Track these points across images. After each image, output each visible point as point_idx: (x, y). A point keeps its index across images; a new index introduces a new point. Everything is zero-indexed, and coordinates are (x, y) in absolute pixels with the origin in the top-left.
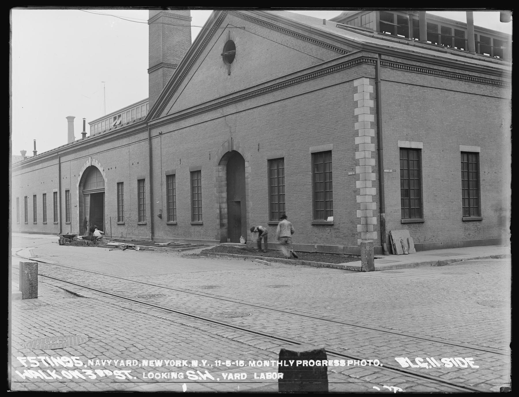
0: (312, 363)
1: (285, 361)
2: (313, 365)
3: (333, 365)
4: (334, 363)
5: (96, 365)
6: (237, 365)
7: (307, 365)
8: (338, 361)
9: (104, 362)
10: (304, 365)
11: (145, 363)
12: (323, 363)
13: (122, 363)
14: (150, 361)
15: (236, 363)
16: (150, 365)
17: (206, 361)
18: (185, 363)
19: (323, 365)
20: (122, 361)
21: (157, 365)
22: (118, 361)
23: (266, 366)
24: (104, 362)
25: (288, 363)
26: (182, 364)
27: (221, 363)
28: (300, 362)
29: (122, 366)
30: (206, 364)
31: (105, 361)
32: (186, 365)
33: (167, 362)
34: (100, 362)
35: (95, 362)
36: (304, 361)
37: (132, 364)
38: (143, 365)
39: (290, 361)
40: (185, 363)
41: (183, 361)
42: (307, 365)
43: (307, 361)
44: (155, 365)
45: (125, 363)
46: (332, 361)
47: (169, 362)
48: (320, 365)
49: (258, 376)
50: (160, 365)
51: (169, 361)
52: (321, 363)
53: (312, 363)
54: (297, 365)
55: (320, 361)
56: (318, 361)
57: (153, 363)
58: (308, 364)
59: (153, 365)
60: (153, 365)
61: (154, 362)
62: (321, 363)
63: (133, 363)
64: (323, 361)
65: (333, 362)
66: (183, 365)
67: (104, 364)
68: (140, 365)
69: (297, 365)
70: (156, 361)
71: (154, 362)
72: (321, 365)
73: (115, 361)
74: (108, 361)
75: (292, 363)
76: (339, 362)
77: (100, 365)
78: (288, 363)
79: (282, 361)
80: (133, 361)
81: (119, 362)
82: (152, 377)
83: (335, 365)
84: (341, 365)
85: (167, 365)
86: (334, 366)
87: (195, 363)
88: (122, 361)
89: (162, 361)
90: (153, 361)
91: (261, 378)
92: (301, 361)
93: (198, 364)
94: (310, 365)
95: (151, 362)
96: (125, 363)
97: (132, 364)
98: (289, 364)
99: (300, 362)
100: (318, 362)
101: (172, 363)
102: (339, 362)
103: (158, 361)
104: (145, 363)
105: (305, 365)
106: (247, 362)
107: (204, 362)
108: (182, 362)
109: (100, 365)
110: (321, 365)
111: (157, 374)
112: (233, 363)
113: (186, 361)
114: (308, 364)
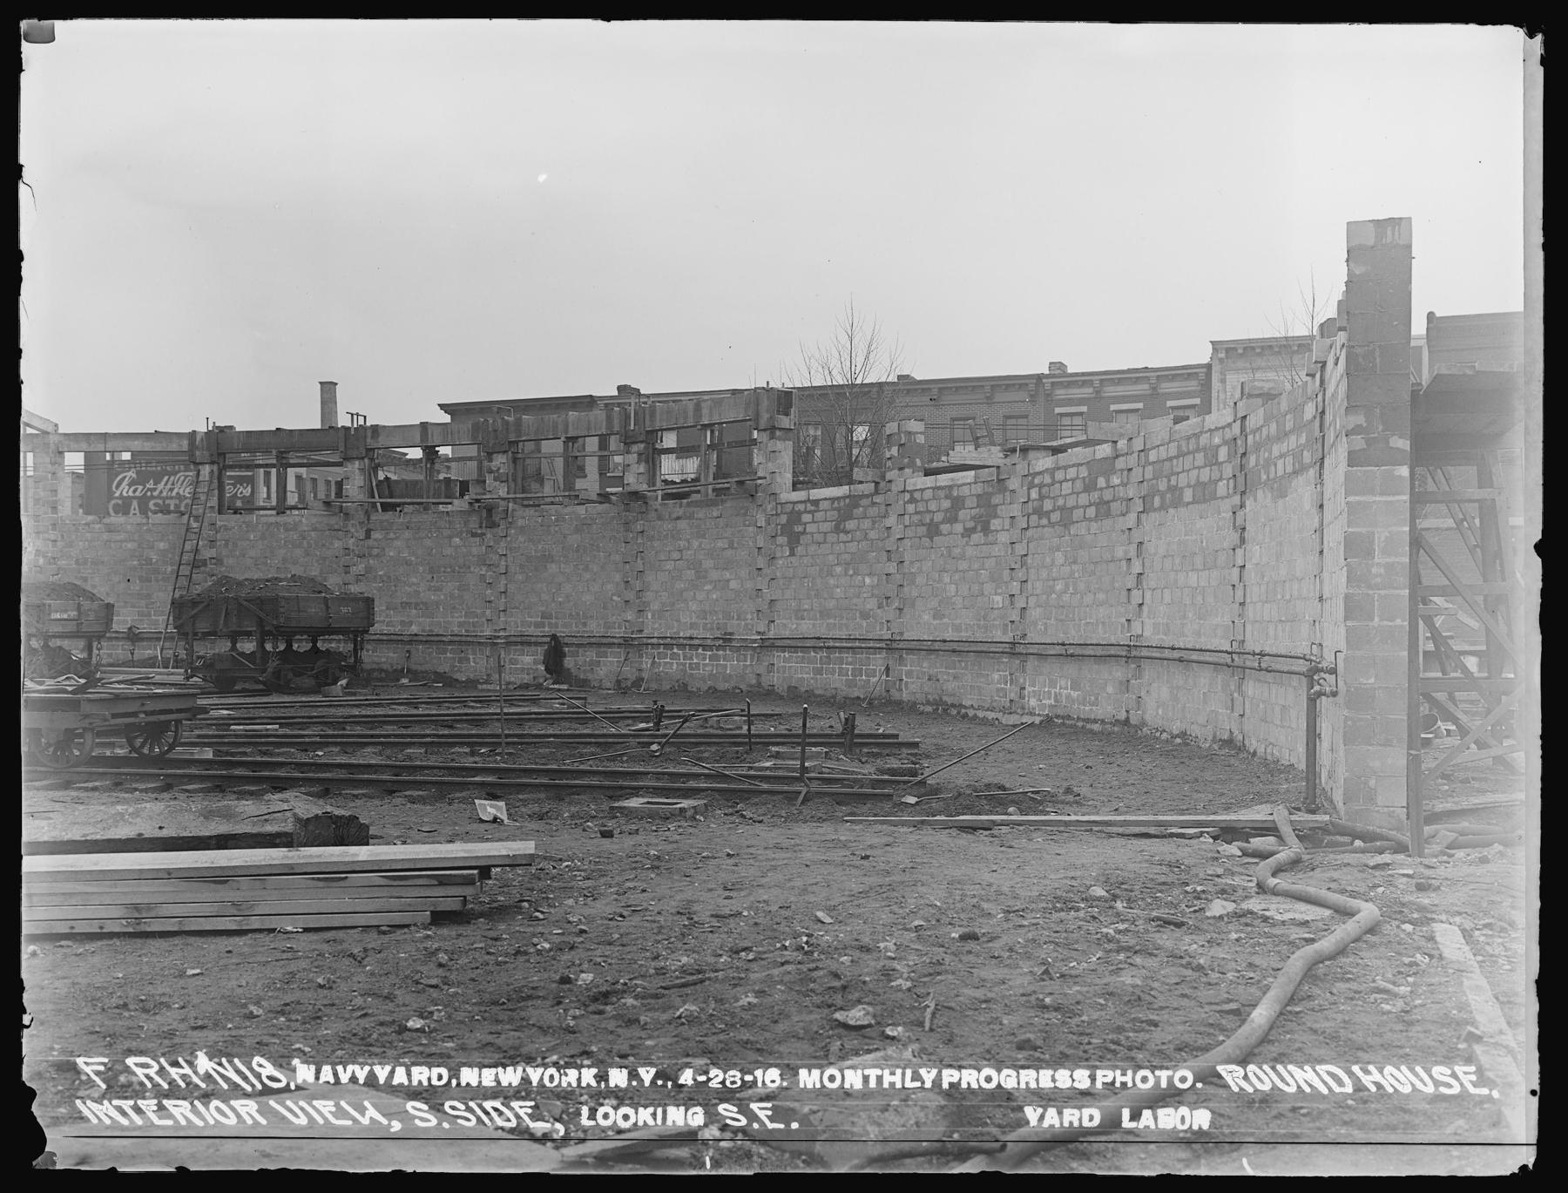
0: (989, 1079)
1: (909, 1073)
2: (993, 1085)
4: (1057, 1077)
6: (760, 1084)
8: (1070, 1073)
9: (345, 1070)
10: (964, 1085)
11: (469, 1076)
14: (485, 1071)
15: (755, 1078)
16: (484, 1084)
17: (653, 1071)
18: (588, 1076)
19: (1023, 1086)
21: (505, 1083)
24: (345, 1070)
25: (916, 1077)
26: (579, 1080)
29: (401, 1085)
30: (653, 1082)
31: (350, 1068)
32: (594, 1083)
34: (336, 1074)
37: (429, 1079)
39: (923, 1072)
40: (588, 1076)
43: (974, 1072)
44: (499, 1082)
45: (409, 1075)
46: (1049, 1072)
49: (592, 1116)
50: (515, 1083)
52: (1018, 1077)
55: (1014, 1073)
56: (1006, 1072)
57: (493, 1078)
60: (494, 1084)
62: (1018, 1077)
65: (1053, 1076)
68: (454, 1082)
70: (500, 1069)
74: (357, 1068)
75: (928, 1076)
76: (1071, 1076)
78: (916, 1077)
79: (899, 1072)
80: (436, 1071)
84: (1076, 1085)
85: (535, 1084)
86: (1055, 1087)
87: (618, 1078)
92: (955, 1073)
93: (630, 1080)
96: (409, 1075)
98: (923, 1083)
102: (1071, 1076)
103: (510, 1069)
104: (469, 1076)
107: (647, 1074)
112: (748, 1078)
113: (594, 1071)
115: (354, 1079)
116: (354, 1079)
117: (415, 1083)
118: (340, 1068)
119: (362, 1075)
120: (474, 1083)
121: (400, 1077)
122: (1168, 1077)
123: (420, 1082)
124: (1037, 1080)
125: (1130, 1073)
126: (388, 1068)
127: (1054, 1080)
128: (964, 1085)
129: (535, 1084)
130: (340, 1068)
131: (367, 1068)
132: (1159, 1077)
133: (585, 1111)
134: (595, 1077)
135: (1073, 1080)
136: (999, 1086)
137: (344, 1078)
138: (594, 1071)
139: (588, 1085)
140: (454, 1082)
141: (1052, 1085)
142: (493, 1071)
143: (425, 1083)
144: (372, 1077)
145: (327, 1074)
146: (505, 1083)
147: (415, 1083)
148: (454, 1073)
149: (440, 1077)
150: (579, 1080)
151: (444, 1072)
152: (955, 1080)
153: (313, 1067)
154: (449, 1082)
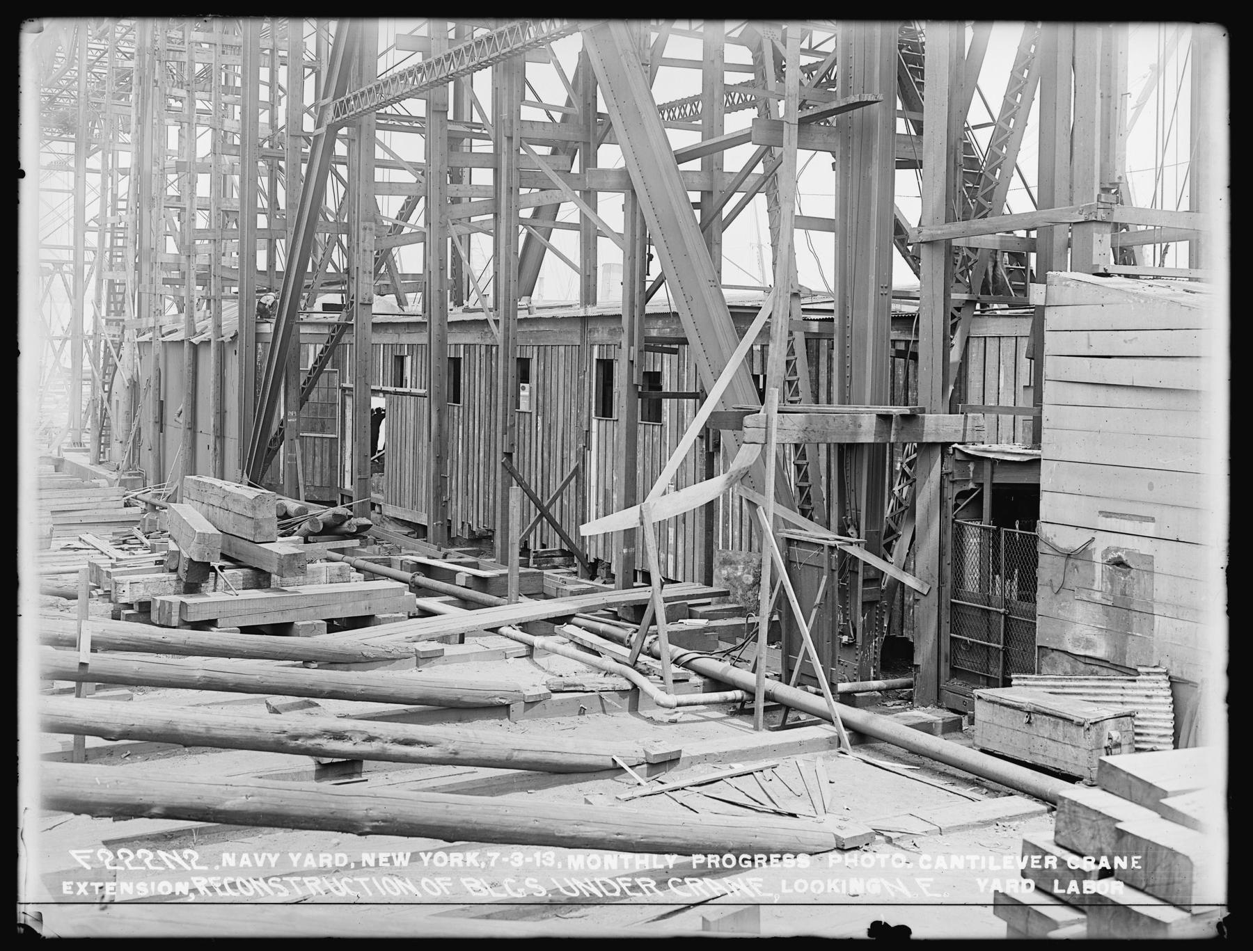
5: (241, 865)
7: (717, 866)
9: (260, 857)
10: (710, 866)
24: (260, 857)
31: (264, 855)
32: (477, 865)
35: (238, 859)
36: (710, 856)
41: (468, 854)
42: (717, 866)
43: (717, 857)
47: (432, 858)
57: (386, 860)
58: (720, 863)
60: (388, 865)
66: (468, 864)
67: (260, 863)
73: (291, 855)
74: (269, 855)
77: (250, 865)
80: (338, 856)
81: (301, 861)
82: (804, 890)
88: (310, 856)
90: (388, 855)
91: (1069, 892)
94: (725, 865)
97: (333, 861)
100: (744, 860)
101: (441, 860)
108: (465, 857)
109: (249, 863)
111: (814, 883)
118: (256, 855)
119: (273, 860)
122: (976, 861)
126: (299, 855)
130: (256, 855)
131: (277, 855)
134: (477, 858)
137: (260, 863)
139: (471, 864)
144: (284, 860)
145: (245, 861)
149: (341, 860)
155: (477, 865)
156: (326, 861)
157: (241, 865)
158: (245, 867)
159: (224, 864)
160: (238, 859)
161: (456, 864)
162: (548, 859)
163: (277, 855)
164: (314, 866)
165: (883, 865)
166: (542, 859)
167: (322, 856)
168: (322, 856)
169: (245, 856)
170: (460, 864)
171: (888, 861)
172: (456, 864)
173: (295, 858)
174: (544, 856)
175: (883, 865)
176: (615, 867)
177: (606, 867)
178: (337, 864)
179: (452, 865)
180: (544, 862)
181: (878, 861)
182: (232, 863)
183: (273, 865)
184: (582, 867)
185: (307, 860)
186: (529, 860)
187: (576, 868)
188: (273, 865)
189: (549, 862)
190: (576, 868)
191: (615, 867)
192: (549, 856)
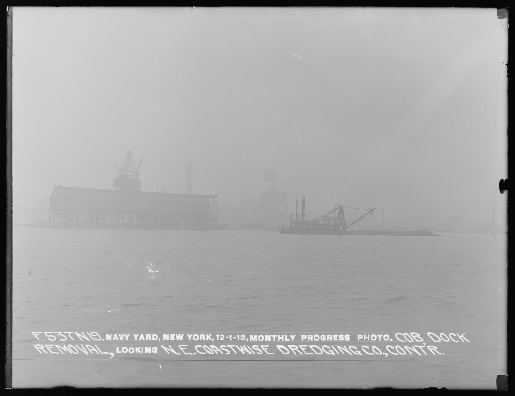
0: (316, 338)
1: (286, 336)
2: (319, 339)
3: (337, 340)
5: (114, 339)
6: (239, 339)
7: (312, 340)
9: (121, 337)
10: (308, 340)
11: (166, 337)
12: (328, 338)
13: (142, 337)
16: (171, 339)
18: (209, 337)
19: (328, 340)
20: (142, 335)
21: (178, 339)
22: (138, 335)
23: (267, 340)
24: (121, 337)
26: (206, 338)
27: (232, 337)
28: (304, 337)
29: (142, 340)
31: (123, 335)
33: (189, 337)
35: (112, 337)
36: (309, 336)
37: (152, 337)
38: (164, 339)
39: (291, 336)
40: (209, 337)
41: (207, 335)
42: (312, 340)
43: (312, 336)
44: (176, 339)
45: (145, 338)
46: (337, 335)
48: (324, 339)
50: (181, 339)
51: (191, 335)
52: (326, 337)
53: (316, 338)
54: (302, 340)
55: (325, 336)
58: (313, 338)
59: (174, 339)
61: (175, 337)
62: (326, 337)
63: (153, 337)
64: (328, 336)
66: (207, 339)
69: (302, 340)
70: (177, 335)
71: (175, 337)
72: (325, 340)
73: (134, 335)
74: (125, 335)
77: (117, 339)
80: (153, 335)
81: (139, 337)
83: (340, 340)
84: (345, 340)
85: (190, 339)
86: (338, 340)
88: (142, 335)
89: (183, 335)
92: (306, 336)
94: (315, 339)
95: (172, 336)
96: (145, 338)
97: (152, 337)
99: (304, 337)
100: (323, 337)
101: (196, 337)
102: (344, 337)
103: (180, 335)
104: (166, 337)
105: (310, 339)
106: (248, 337)
109: (117, 339)
110: (325, 340)
113: (210, 335)
114: (313, 338)
115: (124, 337)
116: (124, 337)
117: (147, 339)
118: (120, 335)
119: (127, 337)
120: (168, 339)
121: (142, 337)
123: (148, 339)
124: (333, 338)
125: (369, 335)
126: (138, 335)
127: (338, 338)
128: (308, 340)
129: (190, 339)
130: (120, 335)
131: (129, 335)
132: (378, 337)
133: (118, 348)
134: (211, 337)
135: (345, 338)
136: (320, 339)
137: (122, 338)
138: (210, 335)
140: (160, 340)
141: (337, 340)
142: (174, 335)
143: (150, 339)
146: (178, 339)
147: (147, 339)
148: (160, 336)
149: (155, 337)
150: (206, 338)
151: (156, 336)
152: (306, 338)
153: (111, 335)
154: (158, 340)
155: (210, 339)
156: (148, 337)
157: (114, 339)
158: (116, 340)
159: (107, 339)
160: (112, 337)
161: (202, 339)
162: (243, 337)
163: (129, 335)
164: (144, 339)
165: (380, 340)
166: (240, 337)
167: (147, 335)
168: (147, 335)
169: (115, 335)
170: (204, 339)
171: (382, 338)
172: (202, 339)
173: (136, 336)
174: (241, 336)
175: (380, 340)
176: (269, 340)
177: (266, 340)
178: (153, 339)
179: (201, 339)
180: (241, 339)
181: (378, 338)
182: (110, 339)
183: (127, 339)
184: (256, 340)
185: (141, 337)
186: (235, 338)
187: (254, 340)
188: (127, 339)
189: (243, 339)
190: (254, 340)
191: (269, 340)
192: (243, 336)
